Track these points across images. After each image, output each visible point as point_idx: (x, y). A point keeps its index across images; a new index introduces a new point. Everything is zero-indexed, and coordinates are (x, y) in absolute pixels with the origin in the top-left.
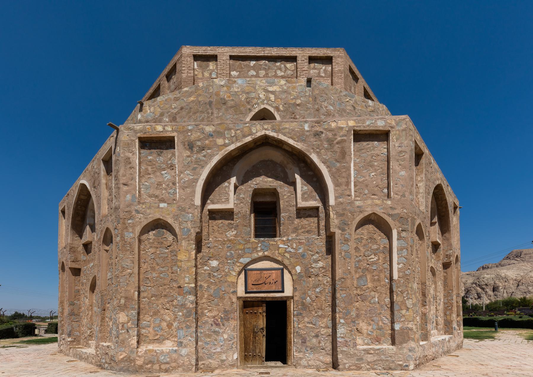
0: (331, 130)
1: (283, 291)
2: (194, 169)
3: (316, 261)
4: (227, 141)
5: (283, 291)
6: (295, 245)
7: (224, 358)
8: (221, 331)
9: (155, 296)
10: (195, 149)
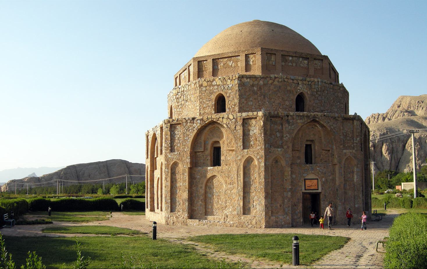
1: (318, 190)
5: (318, 190)
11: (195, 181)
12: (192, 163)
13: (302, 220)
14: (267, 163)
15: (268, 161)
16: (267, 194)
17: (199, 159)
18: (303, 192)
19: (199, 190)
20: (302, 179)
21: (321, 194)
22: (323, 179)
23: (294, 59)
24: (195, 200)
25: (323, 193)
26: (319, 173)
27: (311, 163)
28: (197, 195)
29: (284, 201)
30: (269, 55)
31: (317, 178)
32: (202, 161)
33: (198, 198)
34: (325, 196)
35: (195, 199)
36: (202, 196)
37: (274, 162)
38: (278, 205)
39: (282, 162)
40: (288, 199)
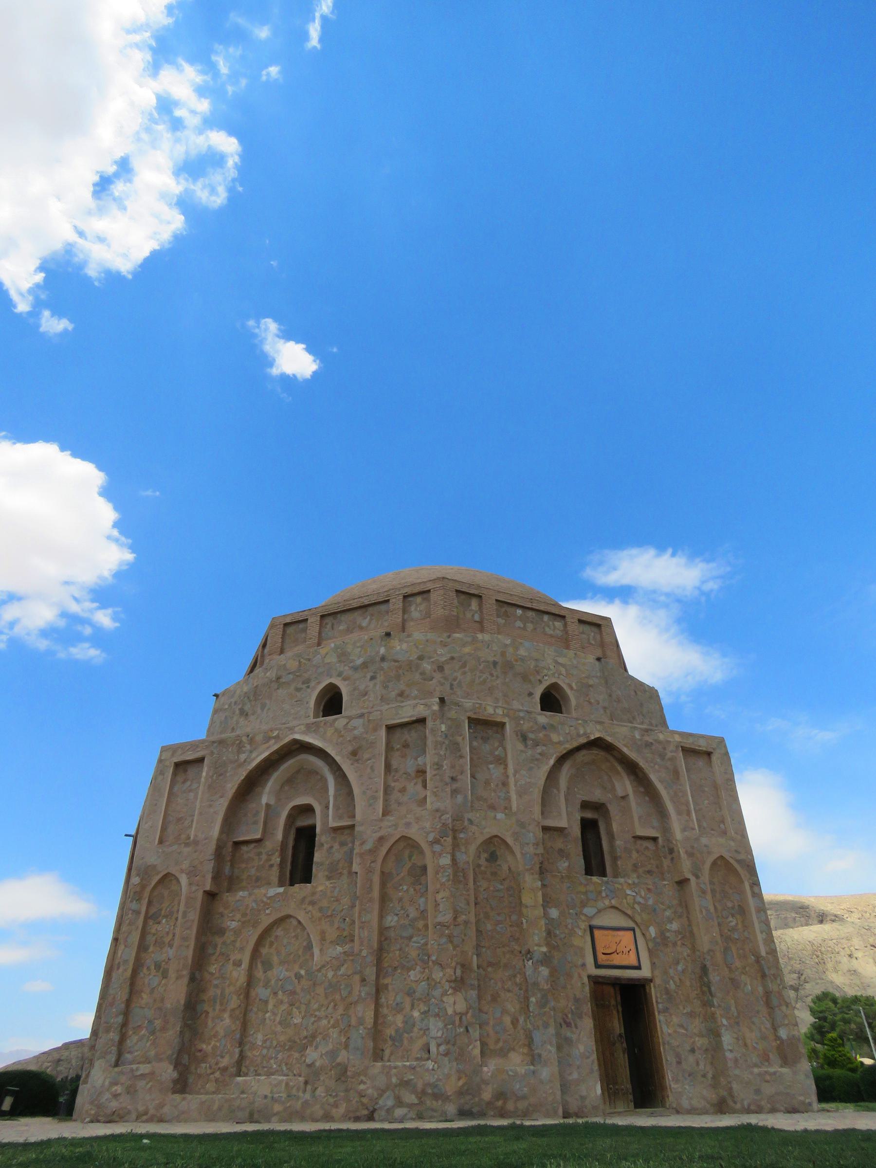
0: (660, 742)
2: (531, 769)
3: (670, 921)
4: (562, 739)
5: (639, 968)
6: (643, 893)
7: (584, 1093)
8: (574, 1037)
9: (490, 964)
10: (530, 743)
11: (219, 940)
12: (217, 877)
13: (599, 1091)
14: (461, 857)
15: (463, 850)
16: (463, 972)
17: (244, 866)
18: (589, 977)
19: (231, 972)
20: (584, 925)
21: (652, 985)
22: (653, 931)
23: (530, 614)
24: (211, 1015)
25: (658, 981)
26: (633, 908)
27: (603, 874)
28: (219, 992)
29: (527, 999)
30: (463, 597)
31: (631, 924)
32: (253, 871)
33: (221, 1004)
34: (667, 991)
35: (210, 1010)
36: (235, 997)
37: (484, 856)
38: (507, 1020)
39: (510, 858)
40: (539, 995)
